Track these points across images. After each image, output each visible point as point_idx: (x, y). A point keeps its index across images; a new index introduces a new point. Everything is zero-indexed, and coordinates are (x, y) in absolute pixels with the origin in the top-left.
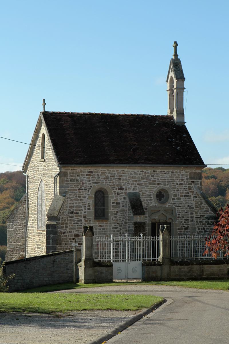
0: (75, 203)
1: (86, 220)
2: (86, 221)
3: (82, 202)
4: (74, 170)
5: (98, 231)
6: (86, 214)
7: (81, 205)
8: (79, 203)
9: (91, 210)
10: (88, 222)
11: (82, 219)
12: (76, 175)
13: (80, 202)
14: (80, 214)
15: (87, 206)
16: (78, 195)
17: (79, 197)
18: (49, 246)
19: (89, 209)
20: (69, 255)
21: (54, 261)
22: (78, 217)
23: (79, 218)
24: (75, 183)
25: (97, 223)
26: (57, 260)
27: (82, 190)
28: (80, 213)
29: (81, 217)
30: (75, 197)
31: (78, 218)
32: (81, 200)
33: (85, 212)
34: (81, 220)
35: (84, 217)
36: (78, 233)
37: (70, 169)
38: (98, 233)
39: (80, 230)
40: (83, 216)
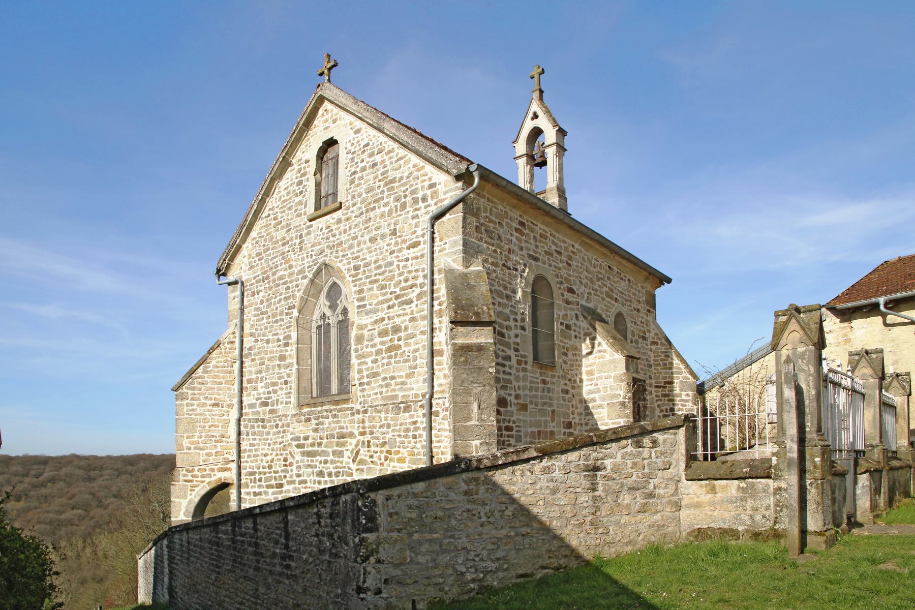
0: (497, 303)
1: (520, 358)
2: (519, 362)
3: (510, 304)
4: (493, 202)
5: (539, 394)
6: (518, 340)
7: (507, 311)
8: (505, 306)
9: (527, 333)
10: (523, 365)
11: (511, 353)
12: (497, 221)
13: (507, 302)
14: (506, 340)
15: (519, 317)
16: (501, 282)
17: (505, 288)
18: (468, 424)
19: (523, 328)
20: (655, 443)
21: (596, 469)
22: (503, 346)
23: (505, 349)
24: (494, 242)
25: (539, 370)
26: (608, 463)
27: (509, 269)
28: (506, 336)
29: (510, 349)
30: (496, 284)
31: (503, 351)
32: (508, 297)
33: (516, 336)
34: (508, 358)
35: (516, 350)
36: (505, 396)
37: (484, 197)
38: (540, 400)
39: (509, 385)
40: (512, 346)
